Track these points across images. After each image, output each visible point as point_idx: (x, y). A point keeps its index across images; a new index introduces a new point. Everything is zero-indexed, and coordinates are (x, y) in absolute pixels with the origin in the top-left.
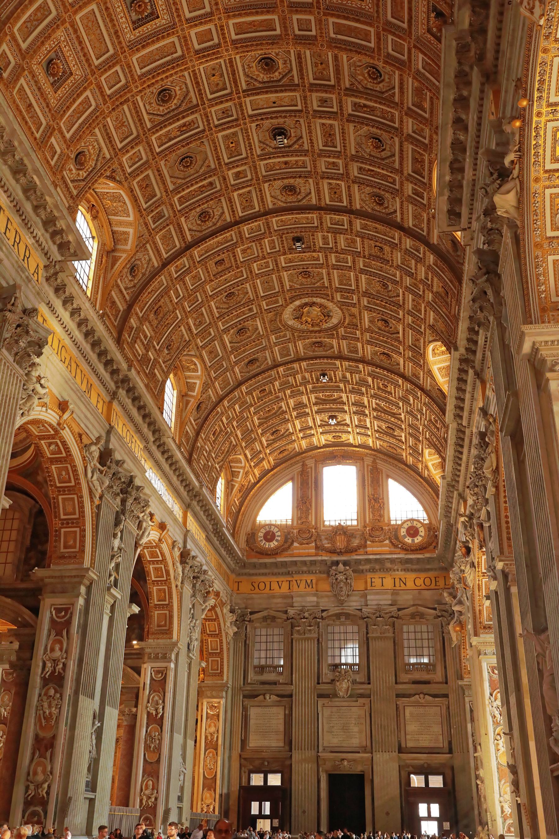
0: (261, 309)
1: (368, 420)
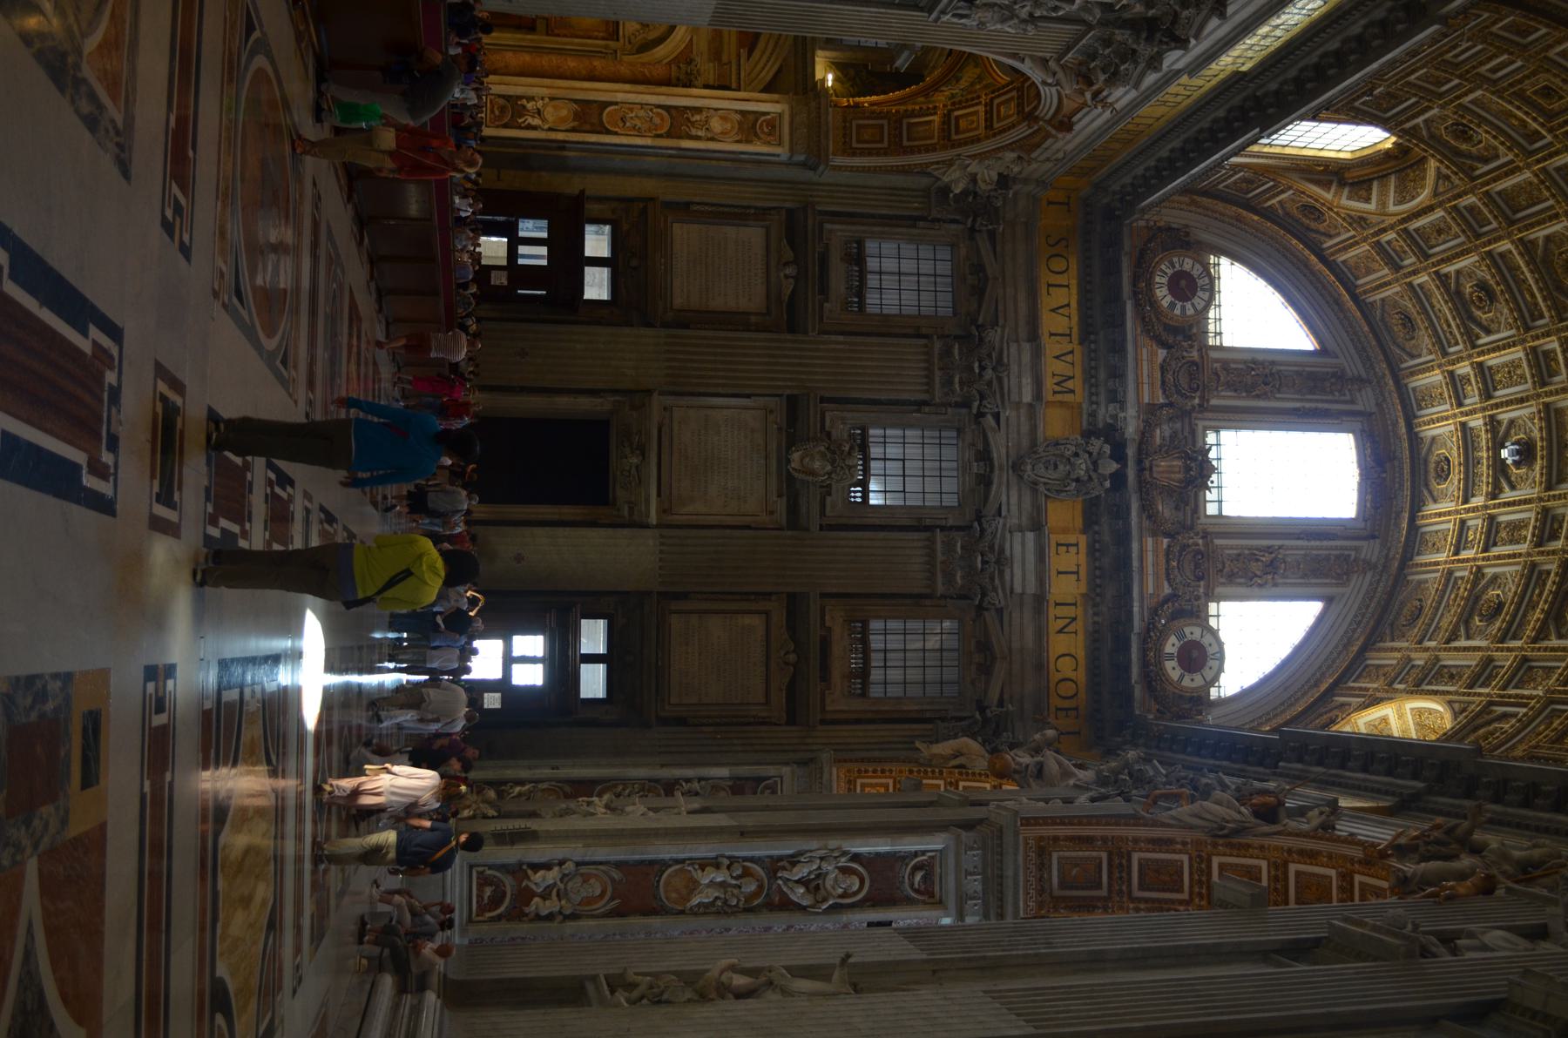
1: (1523, 548)
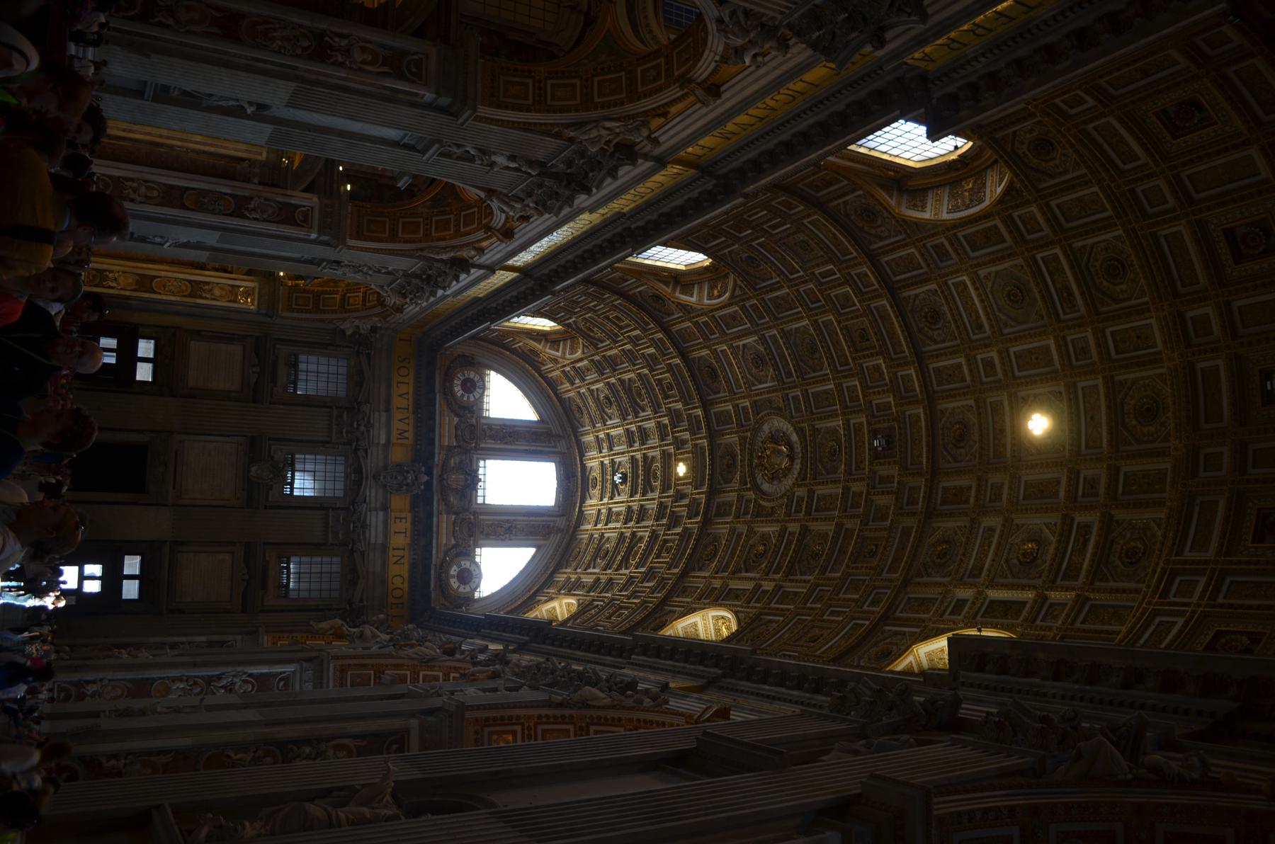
0: (790, 388)
1: (618, 525)
